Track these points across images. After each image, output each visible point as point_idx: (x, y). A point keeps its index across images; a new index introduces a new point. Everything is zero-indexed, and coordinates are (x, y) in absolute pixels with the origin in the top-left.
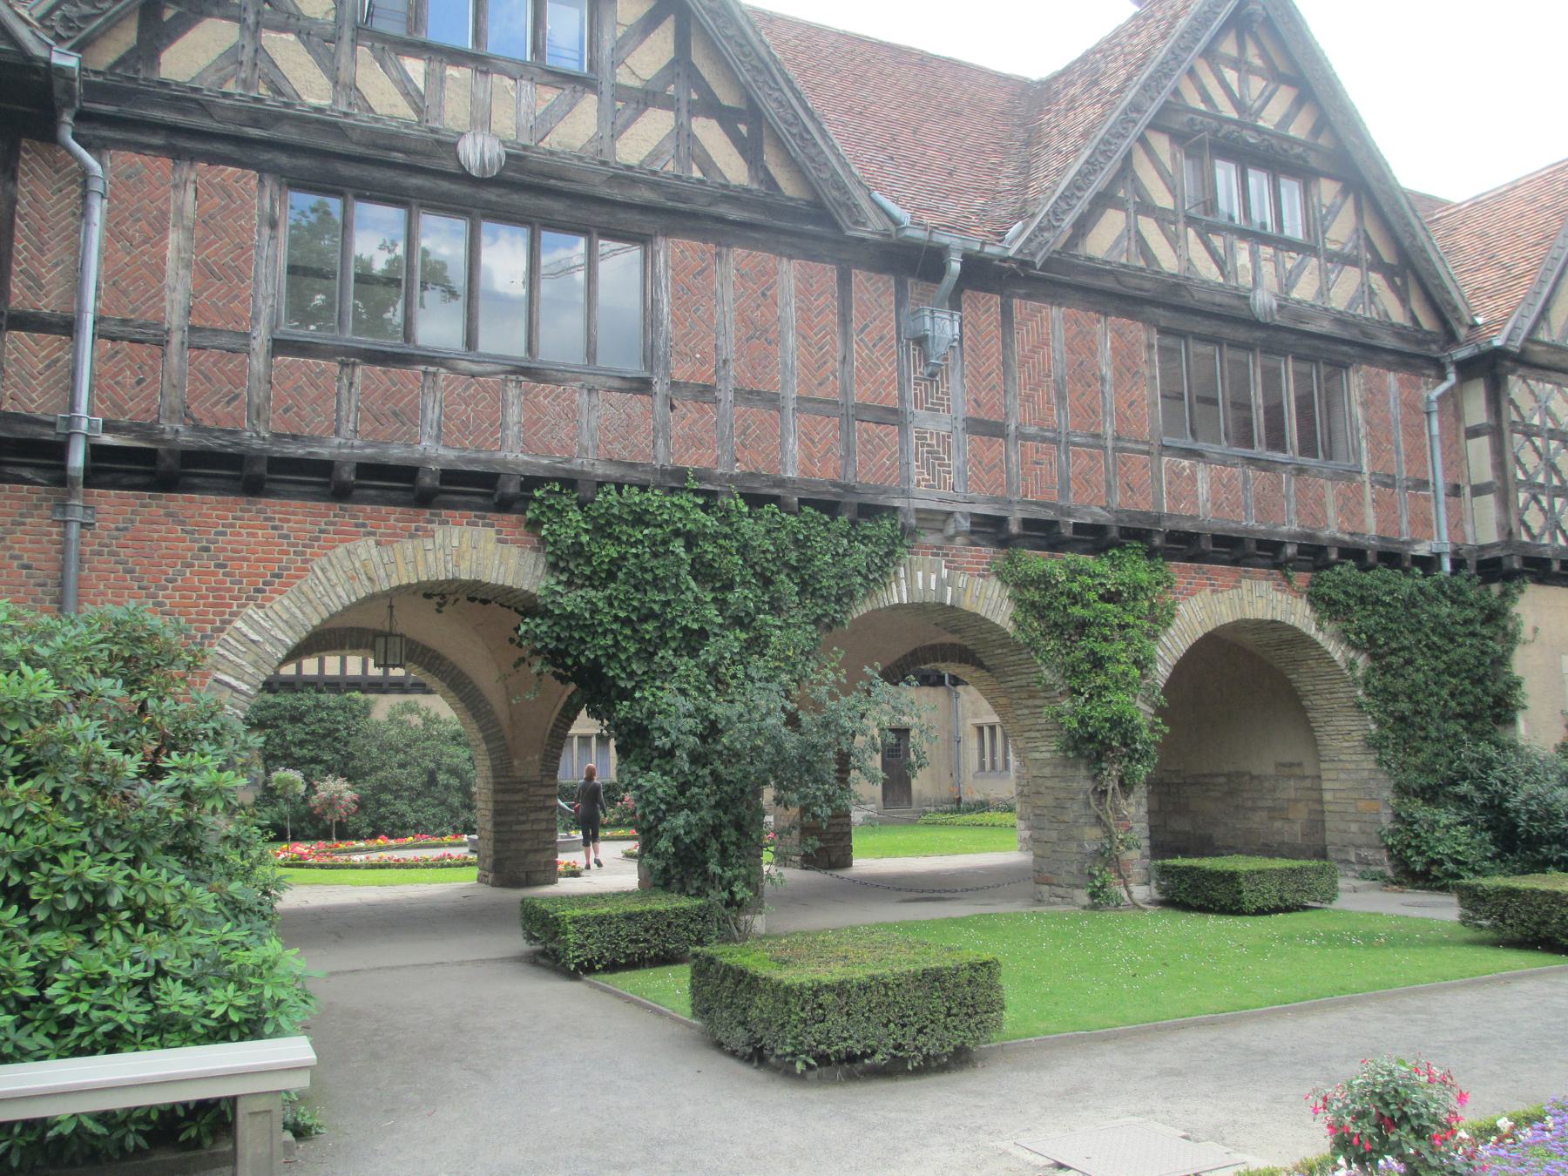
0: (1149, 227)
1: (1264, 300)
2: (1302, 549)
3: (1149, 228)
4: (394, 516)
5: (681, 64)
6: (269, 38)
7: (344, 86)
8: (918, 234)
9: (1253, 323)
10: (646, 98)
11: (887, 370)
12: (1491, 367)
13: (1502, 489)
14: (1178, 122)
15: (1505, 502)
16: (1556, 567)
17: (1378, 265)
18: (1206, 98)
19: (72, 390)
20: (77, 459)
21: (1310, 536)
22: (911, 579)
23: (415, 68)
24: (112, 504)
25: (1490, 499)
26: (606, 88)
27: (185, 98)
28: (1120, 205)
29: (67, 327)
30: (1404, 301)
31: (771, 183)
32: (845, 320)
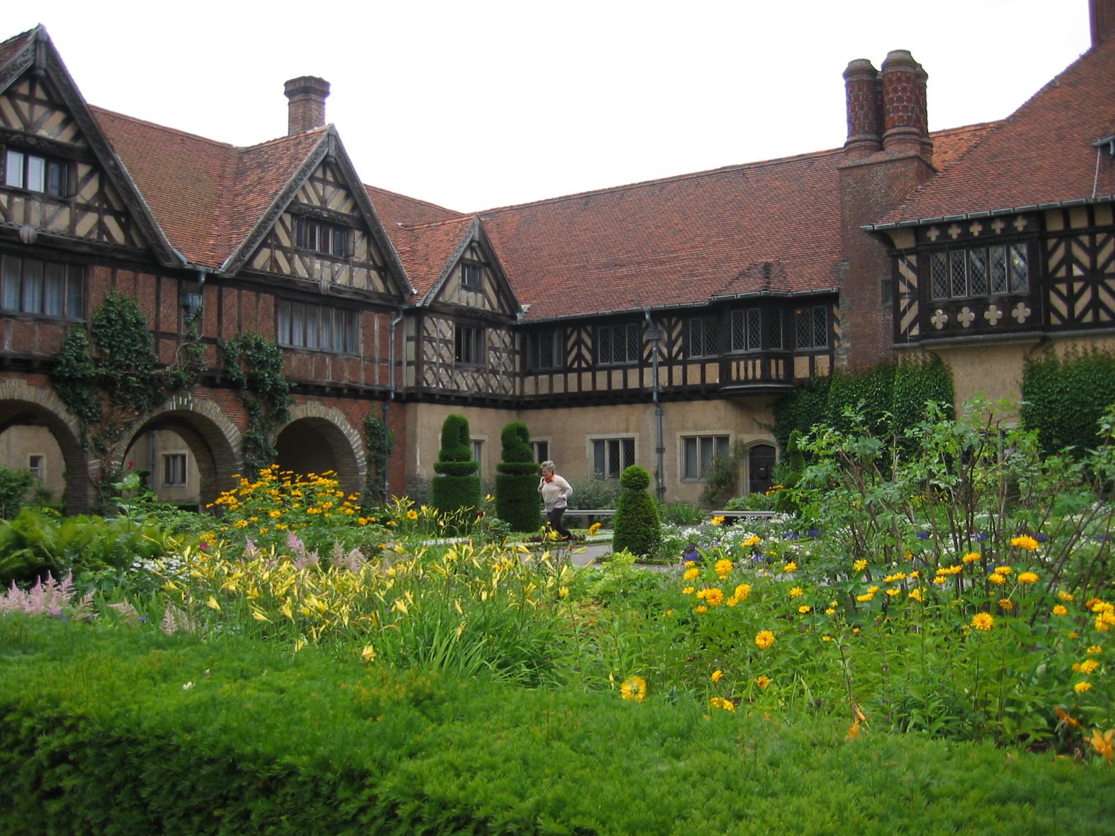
0: (279, 255)
1: (325, 285)
2: (332, 389)
3: (279, 255)
5: (100, 195)
8: (189, 267)
9: (319, 295)
10: (87, 208)
11: (174, 318)
12: (418, 314)
13: (418, 363)
14: (295, 209)
15: (419, 371)
16: (437, 397)
17: (376, 267)
18: (308, 197)
21: (336, 383)
22: (177, 400)
25: (413, 368)
26: (73, 205)
28: (268, 246)
30: (385, 283)
31: (132, 242)
32: (158, 298)
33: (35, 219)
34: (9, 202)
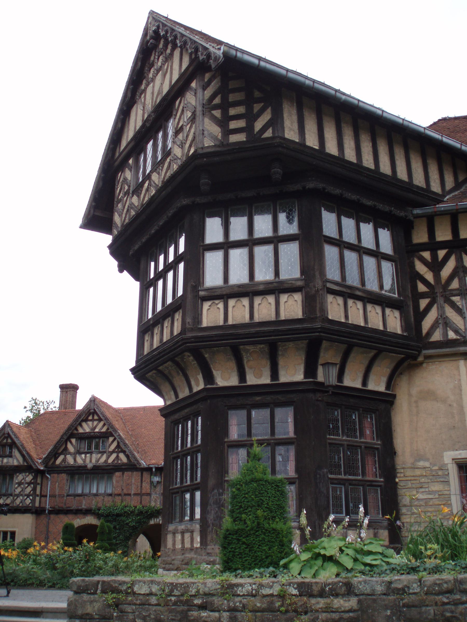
4: (81, 516)
5: (118, 446)
6: (67, 456)
7: (75, 460)
8: (147, 466)
10: (113, 452)
11: (148, 487)
19: (46, 503)
20: (47, 512)
23: (83, 456)
24: (52, 516)
27: (58, 466)
29: (46, 496)
33: (94, 461)
34: (85, 457)
